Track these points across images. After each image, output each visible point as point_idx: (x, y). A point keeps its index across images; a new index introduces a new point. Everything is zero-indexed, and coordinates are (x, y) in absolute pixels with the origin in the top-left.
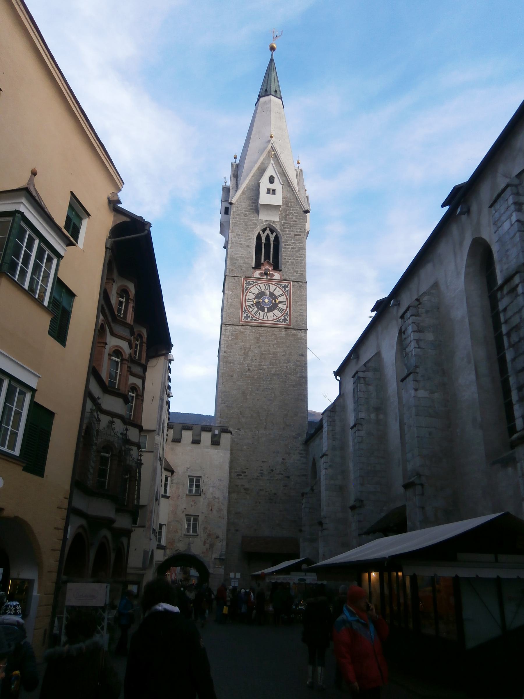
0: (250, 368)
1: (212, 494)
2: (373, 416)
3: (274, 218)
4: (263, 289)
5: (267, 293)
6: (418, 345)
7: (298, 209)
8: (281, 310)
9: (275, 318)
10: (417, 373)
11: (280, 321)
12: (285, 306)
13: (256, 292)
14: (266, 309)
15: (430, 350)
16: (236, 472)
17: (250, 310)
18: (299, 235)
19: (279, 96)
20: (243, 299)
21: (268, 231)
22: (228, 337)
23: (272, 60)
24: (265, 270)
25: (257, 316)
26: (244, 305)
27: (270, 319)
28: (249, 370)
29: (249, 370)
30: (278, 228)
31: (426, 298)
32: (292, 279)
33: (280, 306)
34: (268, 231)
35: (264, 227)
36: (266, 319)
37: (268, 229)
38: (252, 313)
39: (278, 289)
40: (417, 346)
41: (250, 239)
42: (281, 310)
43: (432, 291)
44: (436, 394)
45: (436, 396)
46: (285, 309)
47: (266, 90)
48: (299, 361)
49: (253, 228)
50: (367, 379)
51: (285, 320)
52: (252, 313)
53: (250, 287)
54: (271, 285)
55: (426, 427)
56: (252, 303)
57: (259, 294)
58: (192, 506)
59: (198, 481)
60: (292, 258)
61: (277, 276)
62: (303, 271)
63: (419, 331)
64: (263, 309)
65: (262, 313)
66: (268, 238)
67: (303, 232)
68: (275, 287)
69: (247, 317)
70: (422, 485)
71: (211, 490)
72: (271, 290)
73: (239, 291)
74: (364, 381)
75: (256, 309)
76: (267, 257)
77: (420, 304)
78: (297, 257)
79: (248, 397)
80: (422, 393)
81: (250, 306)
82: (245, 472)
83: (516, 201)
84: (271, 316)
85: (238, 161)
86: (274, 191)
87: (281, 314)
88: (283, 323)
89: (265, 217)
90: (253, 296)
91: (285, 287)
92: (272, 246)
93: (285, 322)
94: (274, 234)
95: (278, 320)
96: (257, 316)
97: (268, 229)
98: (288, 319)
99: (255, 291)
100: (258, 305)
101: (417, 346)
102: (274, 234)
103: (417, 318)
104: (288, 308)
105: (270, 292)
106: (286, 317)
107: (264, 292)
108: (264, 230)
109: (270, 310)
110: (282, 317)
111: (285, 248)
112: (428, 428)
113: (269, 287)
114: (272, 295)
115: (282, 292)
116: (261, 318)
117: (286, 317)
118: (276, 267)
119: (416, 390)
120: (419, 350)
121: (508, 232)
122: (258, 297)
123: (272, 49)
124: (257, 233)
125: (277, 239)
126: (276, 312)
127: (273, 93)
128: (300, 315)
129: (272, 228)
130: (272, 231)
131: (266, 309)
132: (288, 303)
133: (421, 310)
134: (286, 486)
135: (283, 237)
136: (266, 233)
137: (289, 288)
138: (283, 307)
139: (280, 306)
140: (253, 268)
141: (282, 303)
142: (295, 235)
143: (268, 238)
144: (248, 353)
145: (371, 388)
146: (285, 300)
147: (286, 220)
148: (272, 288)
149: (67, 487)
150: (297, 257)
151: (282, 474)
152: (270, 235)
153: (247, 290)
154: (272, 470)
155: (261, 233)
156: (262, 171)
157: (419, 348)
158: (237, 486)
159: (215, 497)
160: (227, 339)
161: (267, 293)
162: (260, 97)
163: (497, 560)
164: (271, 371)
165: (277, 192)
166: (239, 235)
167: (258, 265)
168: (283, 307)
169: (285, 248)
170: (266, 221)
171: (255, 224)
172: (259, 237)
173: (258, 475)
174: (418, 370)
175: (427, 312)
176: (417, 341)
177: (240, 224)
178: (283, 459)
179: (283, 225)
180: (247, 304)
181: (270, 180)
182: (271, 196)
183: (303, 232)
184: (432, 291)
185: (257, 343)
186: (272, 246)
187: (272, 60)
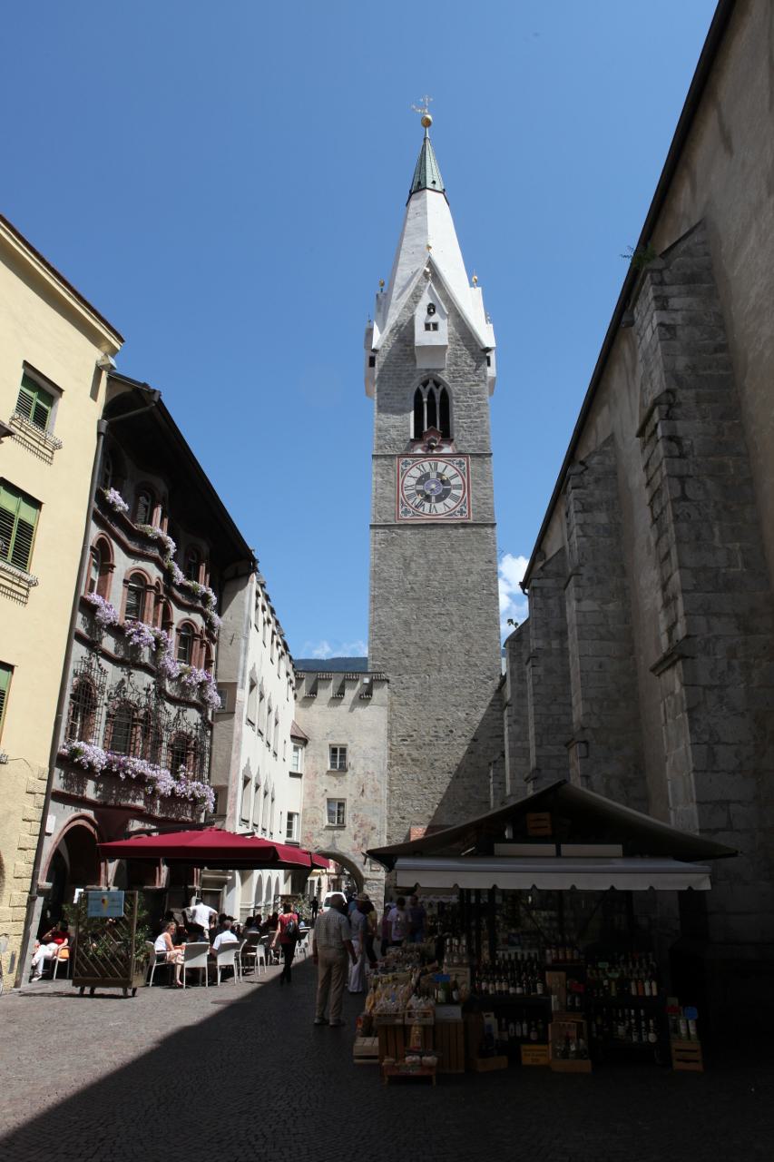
0: (414, 585)
1: (363, 768)
2: (555, 644)
4: (428, 469)
5: (433, 476)
6: (582, 531)
7: (474, 347)
8: (455, 498)
9: (448, 510)
10: (581, 575)
11: (454, 514)
12: (462, 492)
14: (433, 499)
15: (602, 539)
16: (399, 736)
17: (410, 502)
18: (478, 385)
20: (398, 488)
21: (431, 385)
22: (380, 544)
24: (429, 442)
26: (401, 495)
27: (439, 512)
28: (412, 588)
29: (412, 588)
31: (596, 459)
32: (471, 452)
33: (454, 492)
34: (431, 385)
35: (424, 380)
36: (434, 513)
39: (449, 467)
40: (581, 534)
41: (404, 399)
42: (455, 498)
43: (606, 449)
44: (610, 605)
45: (611, 607)
46: (461, 495)
47: (419, 183)
48: (485, 570)
49: (410, 382)
50: (545, 590)
51: (462, 512)
52: (413, 506)
53: (408, 468)
54: (439, 463)
55: (593, 656)
56: (412, 492)
57: (421, 477)
58: (335, 785)
59: (343, 751)
60: (469, 420)
61: (447, 450)
62: (485, 438)
63: (584, 510)
64: (428, 498)
65: (427, 505)
67: (482, 381)
68: (444, 465)
69: (406, 512)
70: (586, 742)
71: (362, 762)
72: (440, 470)
73: (392, 477)
74: (542, 591)
76: (432, 422)
77: (587, 468)
78: (476, 417)
79: (413, 628)
80: (588, 605)
81: (410, 497)
82: (412, 736)
83: (659, 293)
84: (440, 508)
86: (435, 326)
87: (455, 504)
88: (459, 517)
89: (423, 364)
90: (413, 482)
91: (460, 464)
92: (438, 406)
93: (461, 515)
95: (451, 514)
97: (431, 381)
98: (467, 511)
99: (416, 473)
101: (581, 534)
103: (582, 491)
104: (466, 494)
106: (463, 508)
107: (428, 473)
108: (425, 384)
109: (440, 499)
110: (458, 509)
111: (458, 406)
112: (597, 656)
114: (440, 475)
115: (456, 472)
116: (427, 511)
117: (463, 508)
118: (446, 436)
119: (579, 600)
120: (584, 539)
121: (650, 345)
122: (420, 481)
124: (415, 389)
126: (448, 501)
128: (483, 504)
129: (438, 380)
131: (433, 498)
132: (465, 487)
133: (588, 478)
134: (472, 752)
135: (454, 389)
137: (465, 465)
138: (458, 493)
139: (454, 492)
141: (457, 487)
142: (472, 385)
144: (409, 564)
145: (551, 602)
146: (461, 482)
147: (456, 365)
148: (441, 466)
149: (45, 765)
150: (476, 417)
151: (466, 736)
152: (435, 390)
153: (405, 473)
154: (451, 731)
155: (421, 388)
156: (416, 297)
157: (584, 536)
158: (401, 755)
159: (368, 773)
160: (377, 546)
161: (433, 476)
163: (559, 854)
164: (444, 588)
165: (440, 327)
166: (389, 394)
167: (419, 433)
168: (458, 493)
169: (458, 406)
170: (427, 370)
171: (411, 376)
172: (418, 395)
173: (432, 739)
174: (582, 570)
175: (597, 481)
176: (581, 526)
177: (389, 378)
178: (467, 714)
179: (452, 373)
181: (429, 310)
182: (431, 333)
183: (482, 381)
184: (606, 449)
185: (423, 549)
186: (438, 406)
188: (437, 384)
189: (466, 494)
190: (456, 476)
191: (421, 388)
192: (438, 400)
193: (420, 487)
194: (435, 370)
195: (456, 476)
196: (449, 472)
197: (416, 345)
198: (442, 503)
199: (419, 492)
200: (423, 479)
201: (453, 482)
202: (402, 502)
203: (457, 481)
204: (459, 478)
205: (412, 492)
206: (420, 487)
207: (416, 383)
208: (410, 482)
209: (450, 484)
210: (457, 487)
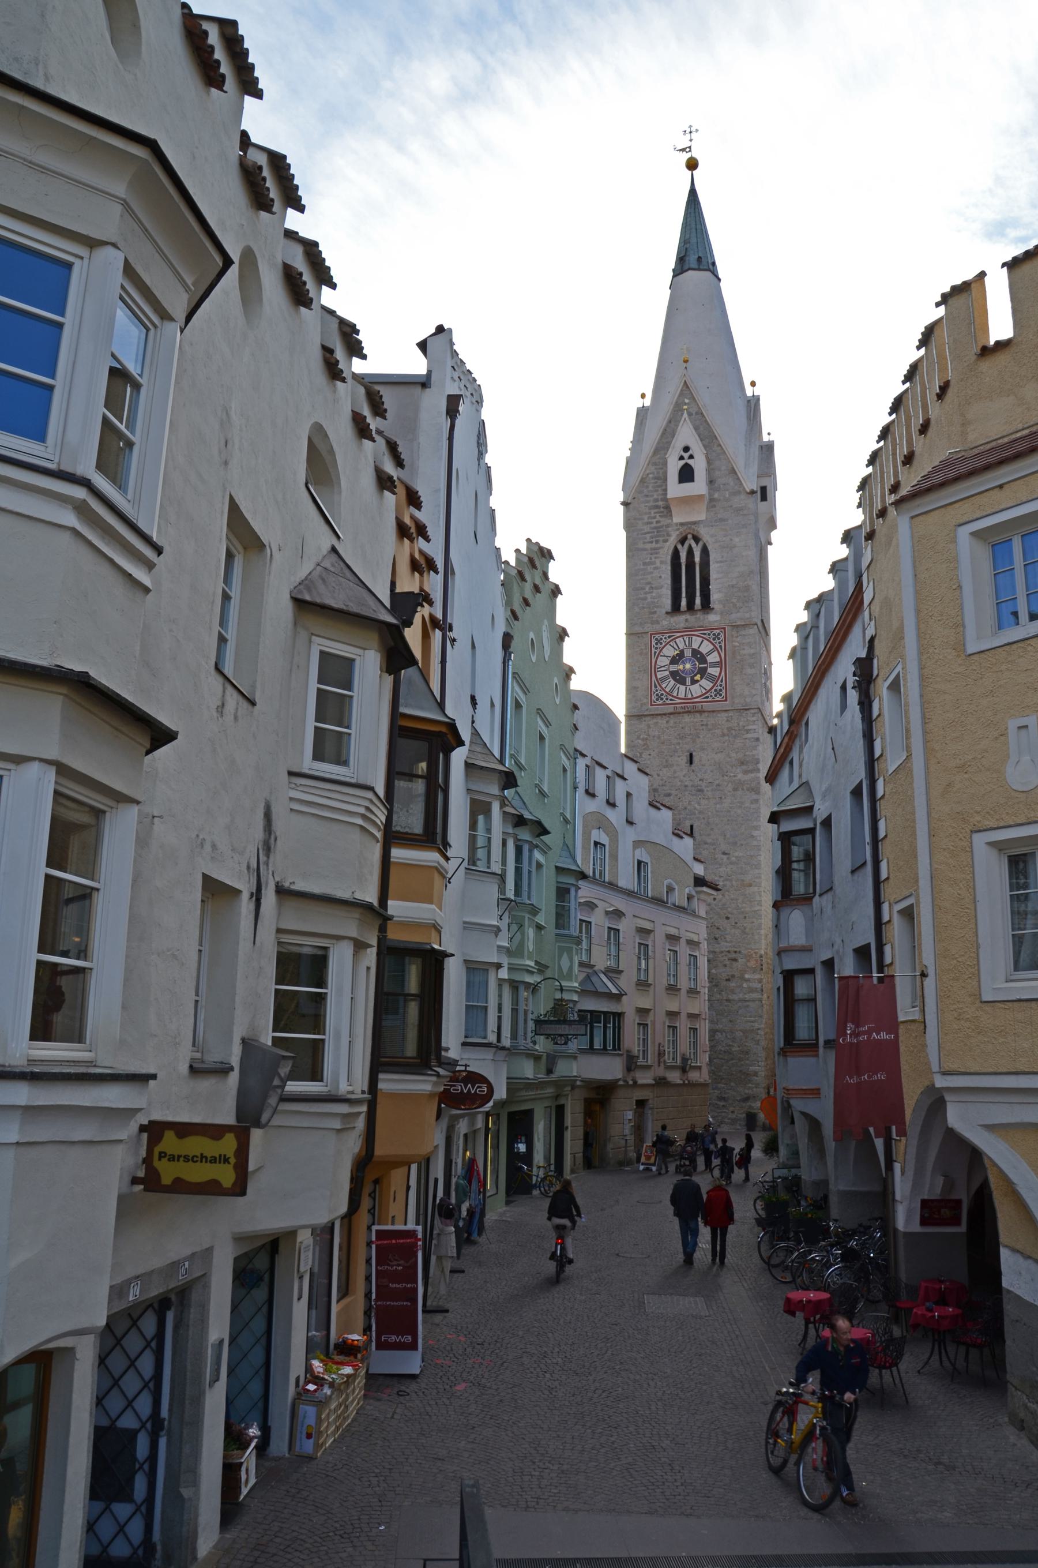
3: (699, 514)
4: (682, 646)
5: (688, 653)
8: (713, 679)
14: (688, 681)
17: (664, 686)
20: (655, 669)
23: (693, 193)
25: (675, 694)
30: (704, 533)
36: (690, 696)
37: (690, 536)
38: (667, 690)
42: (713, 679)
46: (717, 674)
52: (667, 690)
54: (694, 638)
64: (682, 682)
65: (682, 688)
66: (690, 552)
72: (695, 646)
75: (673, 682)
84: (696, 690)
89: (679, 517)
90: (667, 661)
94: (701, 544)
97: (690, 536)
99: (670, 652)
100: (674, 675)
104: (723, 673)
105: (694, 650)
107: (682, 651)
108: (683, 541)
114: (695, 653)
115: (711, 647)
122: (674, 661)
125: (705, 551)
127: (694, 265)
130: (697, 539)
131: (688, 681)
136: (686, 545)
138: (714, 671)
139: (710, 670)
141: (714, 665)
146: (718, 659)
152: (694, 545)
155: (679, 547)
161: (688, 653)
162: (678, 272)
172: (676, 554)
180: (659, 675)
187: (693, 193)
188: (697, 539)
189: (723, 673)
190: (710, 653)
191: (679, 547)
192: (697, 559)
193: (674, 668)
194: (694, 523)
195: (710, 653)
203: (713, 658)
206: (674, 668)
207: (673, 539)
208: (663, 661)
209: (705, 662)
210: (714, 665)
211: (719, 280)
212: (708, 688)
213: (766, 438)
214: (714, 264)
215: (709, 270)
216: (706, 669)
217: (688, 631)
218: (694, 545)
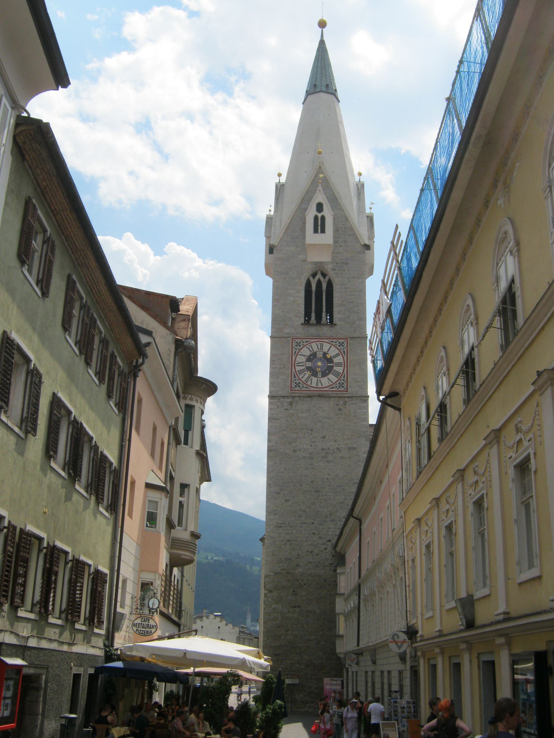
4: (315, 349)
5: (320, 355)
8: (337, 374)
9: (331, 383)
12: (342, 368)
13: (308, 353)
14: (320, 375)
19: (330, 91)
20: (293, 364)
21: (319, 276)
25: (309, 383)
34: (319, 276)
36: (320, 386)
37: (319, 273)
39: (333, 348)
42: (337, 374)
46: (341, 371)
47: (315, 86)
54: (325, 344)
56: (303, 367)
64: (315, 374)
65: (314, 379)
66: (319, 283)
68: (329, 345)
81: (301, 372)
84: (325, 381)
85: (283, 180)
87: (337, 379)
89: (314, 257)
90: (303, 359)
94: (327, 278)
96: (309, 383)
97: (319, 273)
99: (306, 352)
102: (327, 278)
108: (314, 275)
109: (324, 375)
113: (322, 346)
114: (325, 354)
122: (309, 359)
123: (322, 24)
124: (307, 278)
125: (330, 284)
126: (331, 376)
127: (324, 89)
129: (324, 271)
131: (320, 375)
136: (317, 278)
138: (340, 369)
140: (302, 324)
141: (339, 364)
143: (319, 283)
146: (342, 361)
155: (311, 278)
161: (320, 355)
162: (308, 93)
170: (316, 263)
172: (308, 285)
180: (298, 368)
187: (322, 43)
188: (324, 275)
190: (337, 355)
191: (311, 278)
193: (309, 364)
195: (337, 355)
196: (333, 352)
197: (307, 243)
198: (326, 378)
199: (308, 369)
200: (312, 357)
201: (336, 360)
202: (294, 375)
203: (339, 359)
204: (340, 357)
205: (303, 367)
206: (309, 364)
208: (301, 359)
210: (339, 364)
211: (339, 101)
212: (334, 381)
213: (368, 211)
214: (336, 90)
215: (332, 94)
216: (332, 367)
217: (319, 337)
218: (322, 279)
